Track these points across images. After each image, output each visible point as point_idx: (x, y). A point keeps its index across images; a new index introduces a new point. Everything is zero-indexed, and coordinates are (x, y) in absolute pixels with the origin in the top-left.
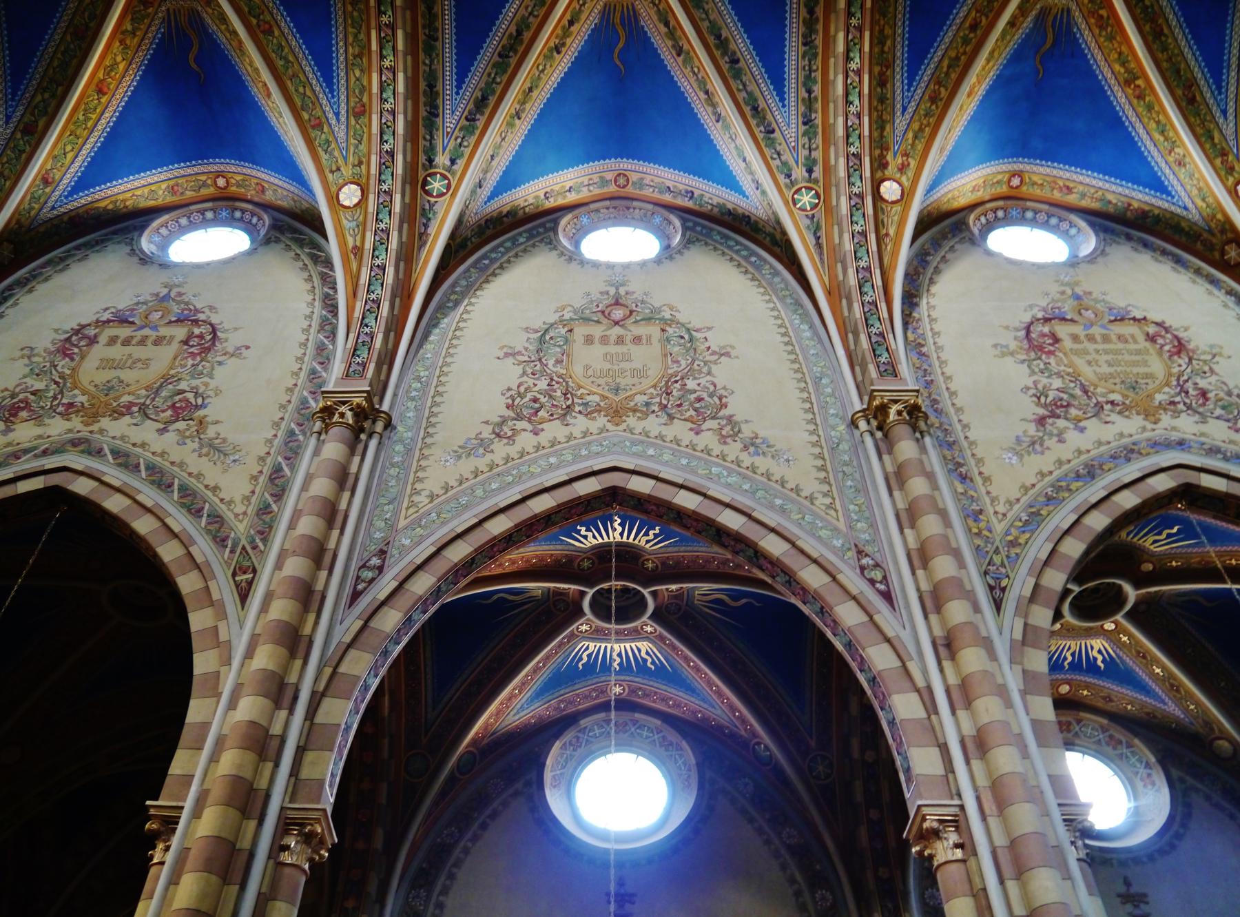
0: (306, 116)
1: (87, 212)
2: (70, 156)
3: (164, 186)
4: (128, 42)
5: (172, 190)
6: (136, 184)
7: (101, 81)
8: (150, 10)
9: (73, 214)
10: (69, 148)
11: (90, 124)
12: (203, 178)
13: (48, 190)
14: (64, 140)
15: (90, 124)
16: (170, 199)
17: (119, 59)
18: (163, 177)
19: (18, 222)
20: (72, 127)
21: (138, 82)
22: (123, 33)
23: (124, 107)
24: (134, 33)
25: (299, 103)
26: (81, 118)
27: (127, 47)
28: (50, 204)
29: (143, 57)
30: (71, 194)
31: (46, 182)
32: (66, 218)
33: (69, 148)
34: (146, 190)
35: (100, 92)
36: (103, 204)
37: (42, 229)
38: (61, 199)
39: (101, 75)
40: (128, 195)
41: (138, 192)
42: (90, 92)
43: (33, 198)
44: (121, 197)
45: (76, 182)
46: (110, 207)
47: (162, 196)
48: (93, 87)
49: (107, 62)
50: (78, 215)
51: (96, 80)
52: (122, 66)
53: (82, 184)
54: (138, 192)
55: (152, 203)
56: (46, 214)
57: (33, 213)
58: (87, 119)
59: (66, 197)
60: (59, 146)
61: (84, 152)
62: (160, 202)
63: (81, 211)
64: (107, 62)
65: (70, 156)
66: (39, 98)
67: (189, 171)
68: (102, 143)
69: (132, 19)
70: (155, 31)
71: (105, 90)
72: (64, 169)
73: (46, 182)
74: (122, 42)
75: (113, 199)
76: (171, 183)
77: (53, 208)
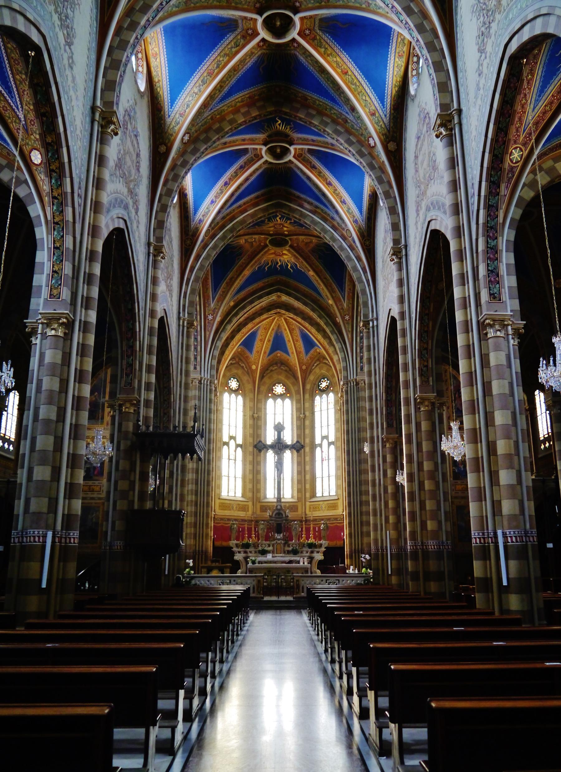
0: (364, 6)
1: (394, 101)
2: (368, 99)
3: (397, 60)
4: (329, 53)
5: (400, 56)
6: (391, 73)
7: (342, 71)
8: (318, 38)
9: (392, 108)
10: (364, 98)
11: (358, 84)
12: (400, 39)
13: (377, 115)
14: (360, 98)
15: (358, 84)
16: (404, 59)
17: (335, 59)
18: (393, 58)
19: (383, 135)
20: (356, 93)
21: (347, 54)
22: (325, 54)
23: (356, 65)
24: (326, 49)
25: (358, 5)
26: (354, 87)
27: (331, 54)
28: (383, 117)
29: (337, 48)
30: (383, 105)
31: (373, 114)
32: (392, 112)
33: (364, 98)
34: (396, 69)
35: (346, 73)
36: (394, 92)
37: (392, 125)
38: (384, 112)
39: (339, 71)
40: (395, 78)
41: (395, 73)
42: (344, 78)
43: (377, 123)
44: (394, 82)
45: (379, 100)
46: (397, 89)
47: (402, 62)
48: (343, 76)
49: (335, 65)
50: (394, 106)
51: (341, 74)
52: (338, 59)
53: (381, 99)
54: (395, 73)
55: (403, 69)
56: (386, 120)
57: (383, 126)
58: (355, 84)
59: (384, 108)
60: (362, 102)
61: (368, 91)
62: (404, 65)
63: (392, 103)
64: (335, 65)
65: (368, 99)
66: (342, 98)
67: (394, 45)
68: (368, 81)
69: (320, 47)
70: (326, 38)
71: (346, 71)
72: (372, 104)
73: (373, 114)
74: (328, 56)
75: (393, 86)
76: (397, 55)
77: (386, 116)
